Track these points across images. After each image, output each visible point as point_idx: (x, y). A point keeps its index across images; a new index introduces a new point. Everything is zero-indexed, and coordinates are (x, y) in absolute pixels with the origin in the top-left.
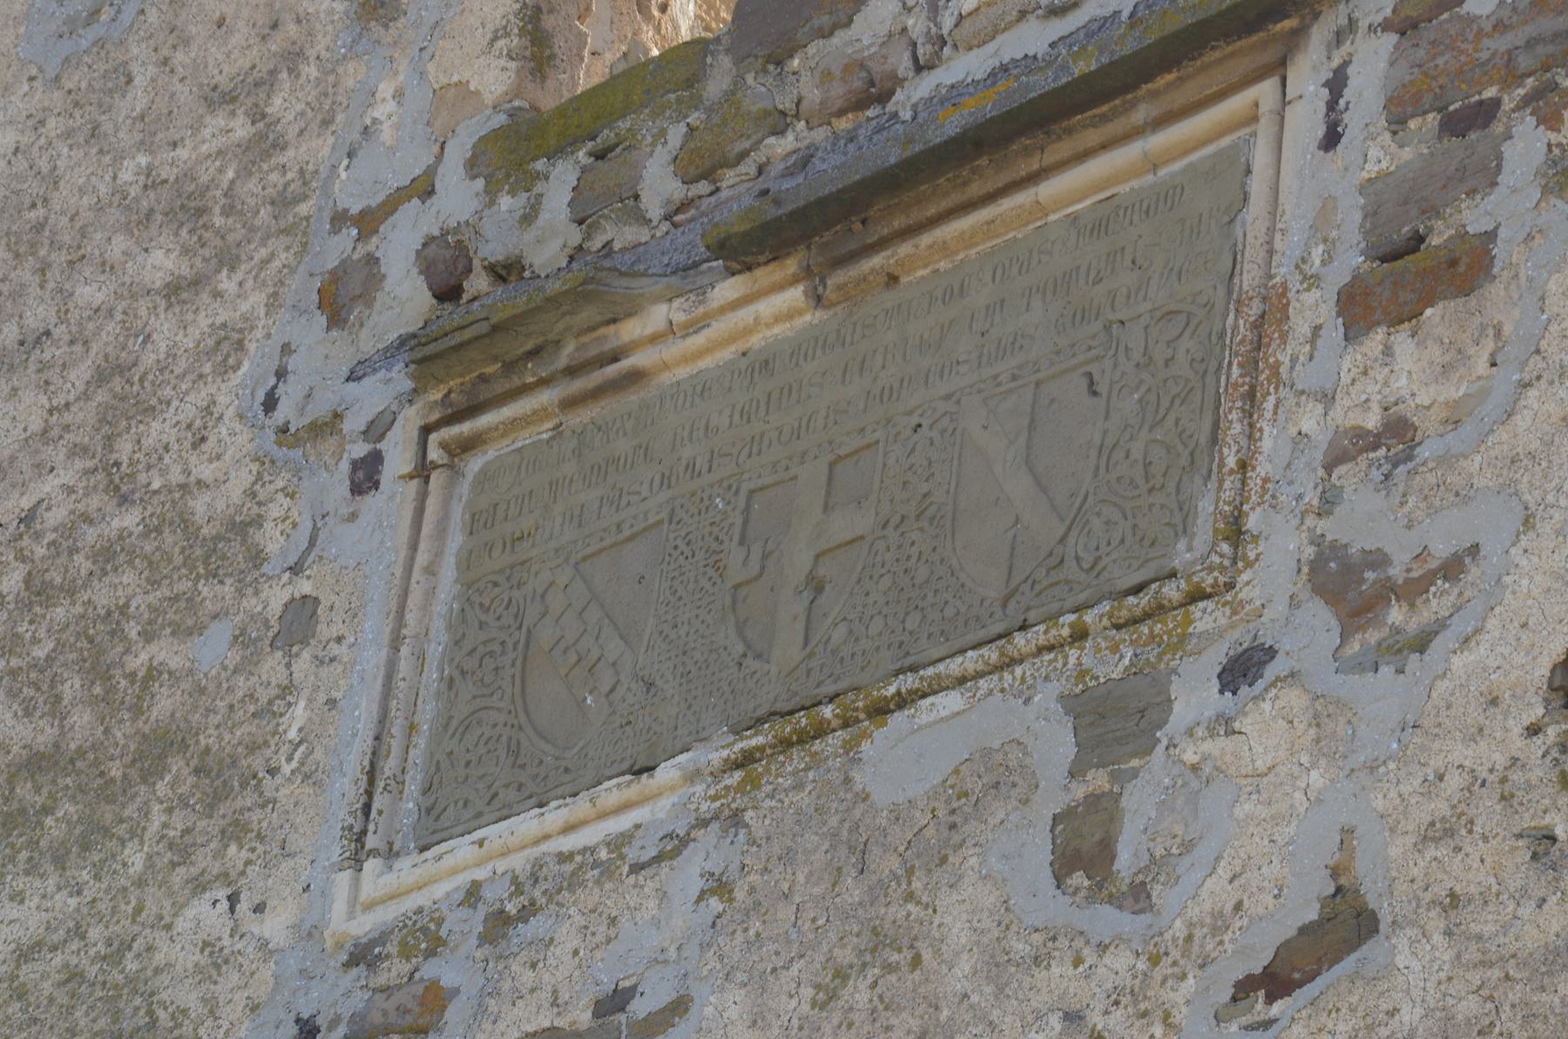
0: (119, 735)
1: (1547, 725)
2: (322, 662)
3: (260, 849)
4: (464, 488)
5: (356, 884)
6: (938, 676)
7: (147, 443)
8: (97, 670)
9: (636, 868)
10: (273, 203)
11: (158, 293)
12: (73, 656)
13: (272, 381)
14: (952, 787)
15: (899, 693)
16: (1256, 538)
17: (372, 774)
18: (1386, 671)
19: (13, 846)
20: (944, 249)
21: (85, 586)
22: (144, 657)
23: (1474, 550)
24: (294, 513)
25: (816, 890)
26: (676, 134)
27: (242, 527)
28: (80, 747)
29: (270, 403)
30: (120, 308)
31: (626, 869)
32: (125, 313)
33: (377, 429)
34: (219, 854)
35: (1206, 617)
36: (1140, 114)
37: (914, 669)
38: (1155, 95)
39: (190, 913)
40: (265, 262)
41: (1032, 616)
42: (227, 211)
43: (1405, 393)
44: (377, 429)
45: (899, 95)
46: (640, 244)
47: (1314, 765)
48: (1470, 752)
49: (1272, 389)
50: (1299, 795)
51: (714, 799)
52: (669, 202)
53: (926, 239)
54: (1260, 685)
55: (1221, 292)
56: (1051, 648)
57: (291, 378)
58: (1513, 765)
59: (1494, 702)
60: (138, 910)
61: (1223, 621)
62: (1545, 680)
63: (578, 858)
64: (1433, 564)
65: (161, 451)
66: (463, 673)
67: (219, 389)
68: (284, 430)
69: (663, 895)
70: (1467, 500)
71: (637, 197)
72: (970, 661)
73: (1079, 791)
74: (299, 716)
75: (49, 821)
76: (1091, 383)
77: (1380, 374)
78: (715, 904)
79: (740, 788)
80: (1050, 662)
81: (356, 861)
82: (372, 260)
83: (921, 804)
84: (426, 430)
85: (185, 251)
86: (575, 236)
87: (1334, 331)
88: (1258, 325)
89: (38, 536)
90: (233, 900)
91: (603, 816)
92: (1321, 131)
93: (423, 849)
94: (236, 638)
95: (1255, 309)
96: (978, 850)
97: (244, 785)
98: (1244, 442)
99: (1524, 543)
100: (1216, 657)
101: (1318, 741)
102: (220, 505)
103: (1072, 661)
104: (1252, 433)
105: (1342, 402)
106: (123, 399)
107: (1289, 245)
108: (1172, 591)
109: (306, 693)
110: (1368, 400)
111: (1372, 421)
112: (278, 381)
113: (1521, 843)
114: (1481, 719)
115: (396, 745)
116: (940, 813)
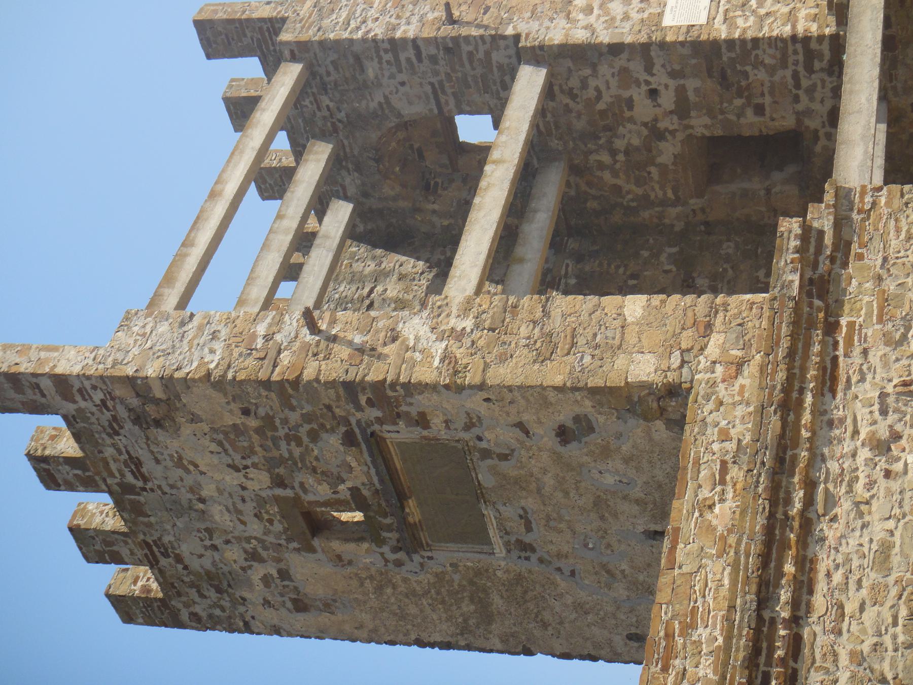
8: (458, 593)
17: (480, 553)
26: (380, 519)
27: (437, 575)
29: (416, 573)
33: (423, 557)
35: (471, 444)
36: (388, 456)
44: (423, 557)
73: (496, 459)
74: (469, 564)
81: (494, 553)
84: (424, 550)
87: (429, 430)
100: (478, 442)
107: (413, 436)
111: (444, 425)
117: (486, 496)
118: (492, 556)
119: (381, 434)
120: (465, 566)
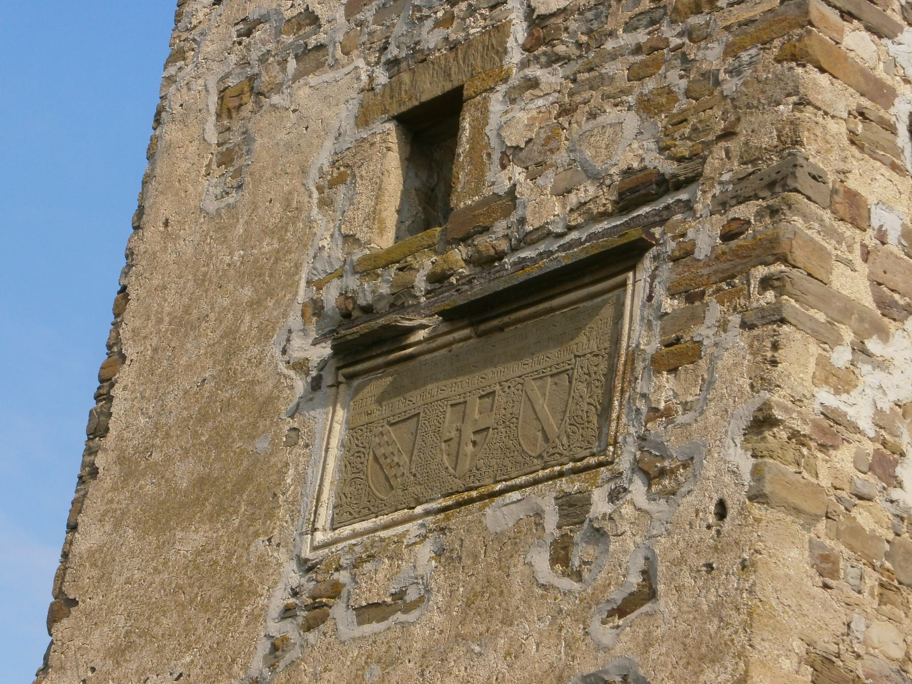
63: (387, 540)
79: (444, 520)
84: (338, 369)
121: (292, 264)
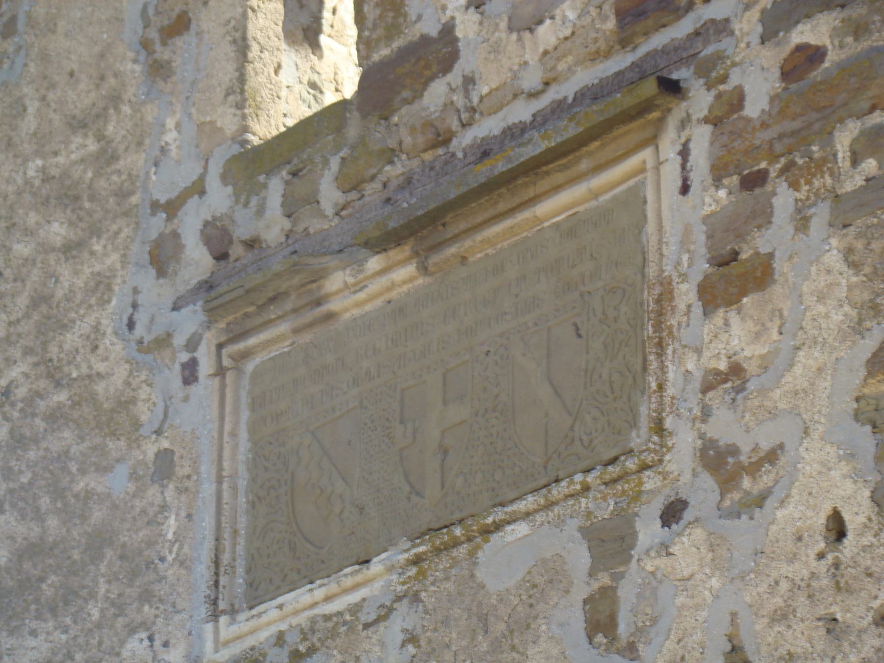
0: (75, 533)
1: (827, 553)
2: (181, 492)
3: (162, 607)
4: (246, 382)
5: (216, 632)
6: (514, 512)
7: (67, 347)
8: (58, 493)
9: (367, 626)
10: (116, 195)
11: (59, 250)
12: (43, 483)
13: (130, 310)
14: (528, 581)
15: (494, 522)
16: (671, 434)
17: (217, 562)
18: (744, 517)
19: (25, 601)
20: (488, 242)
21: (44, 438)
22: (82, 484)
23: (781, 446)
24: (153, 397)
25: (464, 643)
26: (335, 163)
27: (125, 404)
28: (54, 541)
29: (131, 325)
30: (39, 259)
31: (361, 627)
32: (42, 263)
33: (192, 344)
34: (139, 610)
35: (650, 481)
36: (584, 165)
37: (502, 505)
38: (590, 154)
39: (129, 646)
40: (117, 233)
41: (561, 474)
42: (92, 198)
43: (738, 348)
44: (192, 344)
45: (454, 142)
46: (324, 230)
47: (713, 575)
48: (790, 569)
49: (670, 343)
50: (707, 593)
51: (403, 583)
52: (336, 204)
53: (479, 237)
54: (682, 523)
55: (639, 277)
56: (572, 496)
57: (141, 309)
58: (813, 577)
59: (800, 539)
60: (100, 643)
61: (659, 484)
62: (824, 526)
63: (335, 619)
64: (762, 454)
65: (74, 353)
66: (259, 498)
67: (101, 315)
68: (140, 342)
69: (382, 644)
70: (775, 416)
71: (318, 202)
72: (528, 503)
73: (596, 586)
74: (171, 525)
75: (44, 586)
76: (577, 329)
77: (724, 337)
78: (411, 649)
79: (416, 578)
80: (573, 505)
81: (215, 616)
82: (176, 235)
83: (513, 591)
84: (220, 346)
85: (71, 224)
86: (287, 224)
87: (698, 310)
88: (658, 301)
89: (13, 405)
90: (151, 639)
91: (346, 591)
92: (679, 183)
93: (251, 608)
94: (131, 474)
95: (657, 290)
96: (546, 620)
97: (148, 568)
98: (659, 373)
99: (805, 445)
100: (657, 506)
101: (713, 560)
102: (112, 389)
103: (583, 505)
104: (663, 368)
105: (707, 354)
106: (49, 318)
107: (671, 250)
108: (631, 464)
109: (174, 510)
110: (719, 353)
111: (723, 366)
112: (134, 310)
113: (820, 624)
114: (794, 549)
115: (227, 544)
116: (524, 597)
117: (444, 562)
118: (203, 611)
119: (672, 122)
120: (164, 507)
121: (124, 177)
